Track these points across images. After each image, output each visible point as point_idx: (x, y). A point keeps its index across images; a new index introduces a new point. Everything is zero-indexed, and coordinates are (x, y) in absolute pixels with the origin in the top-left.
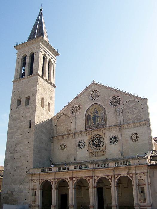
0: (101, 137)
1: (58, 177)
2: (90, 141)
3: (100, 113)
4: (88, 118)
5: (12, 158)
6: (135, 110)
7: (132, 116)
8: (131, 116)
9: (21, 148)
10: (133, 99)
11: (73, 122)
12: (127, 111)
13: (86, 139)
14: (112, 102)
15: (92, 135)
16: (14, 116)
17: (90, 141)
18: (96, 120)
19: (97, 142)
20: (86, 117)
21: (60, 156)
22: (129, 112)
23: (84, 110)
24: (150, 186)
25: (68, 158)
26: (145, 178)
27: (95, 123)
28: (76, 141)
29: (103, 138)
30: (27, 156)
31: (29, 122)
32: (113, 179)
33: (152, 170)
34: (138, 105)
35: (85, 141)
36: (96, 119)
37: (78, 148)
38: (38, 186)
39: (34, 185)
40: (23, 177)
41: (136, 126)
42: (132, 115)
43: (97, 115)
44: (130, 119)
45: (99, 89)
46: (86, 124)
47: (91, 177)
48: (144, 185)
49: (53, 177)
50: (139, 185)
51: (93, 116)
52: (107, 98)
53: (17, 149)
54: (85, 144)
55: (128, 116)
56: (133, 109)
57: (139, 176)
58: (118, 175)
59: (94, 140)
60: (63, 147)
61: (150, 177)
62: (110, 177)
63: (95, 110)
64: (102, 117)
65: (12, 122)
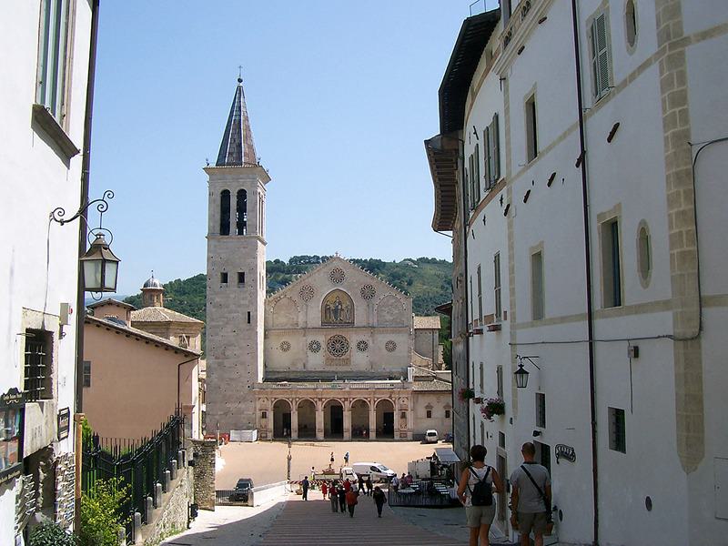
3: (344, 306)
4: (326, 310)
8: (388, 317)
13: (322, 339)
16: (217, 300)
19: (338, 346)
21: (283, 361)
25: (294, 364)
26: (410, 404)
32: (372, 402)
37: (309, 352)
38: (270, 406)
39: (261, 405)
41: (393, 332)
47: (346, 399)
49: (293, 396)
60: (286, 347)
65: (214, 310)
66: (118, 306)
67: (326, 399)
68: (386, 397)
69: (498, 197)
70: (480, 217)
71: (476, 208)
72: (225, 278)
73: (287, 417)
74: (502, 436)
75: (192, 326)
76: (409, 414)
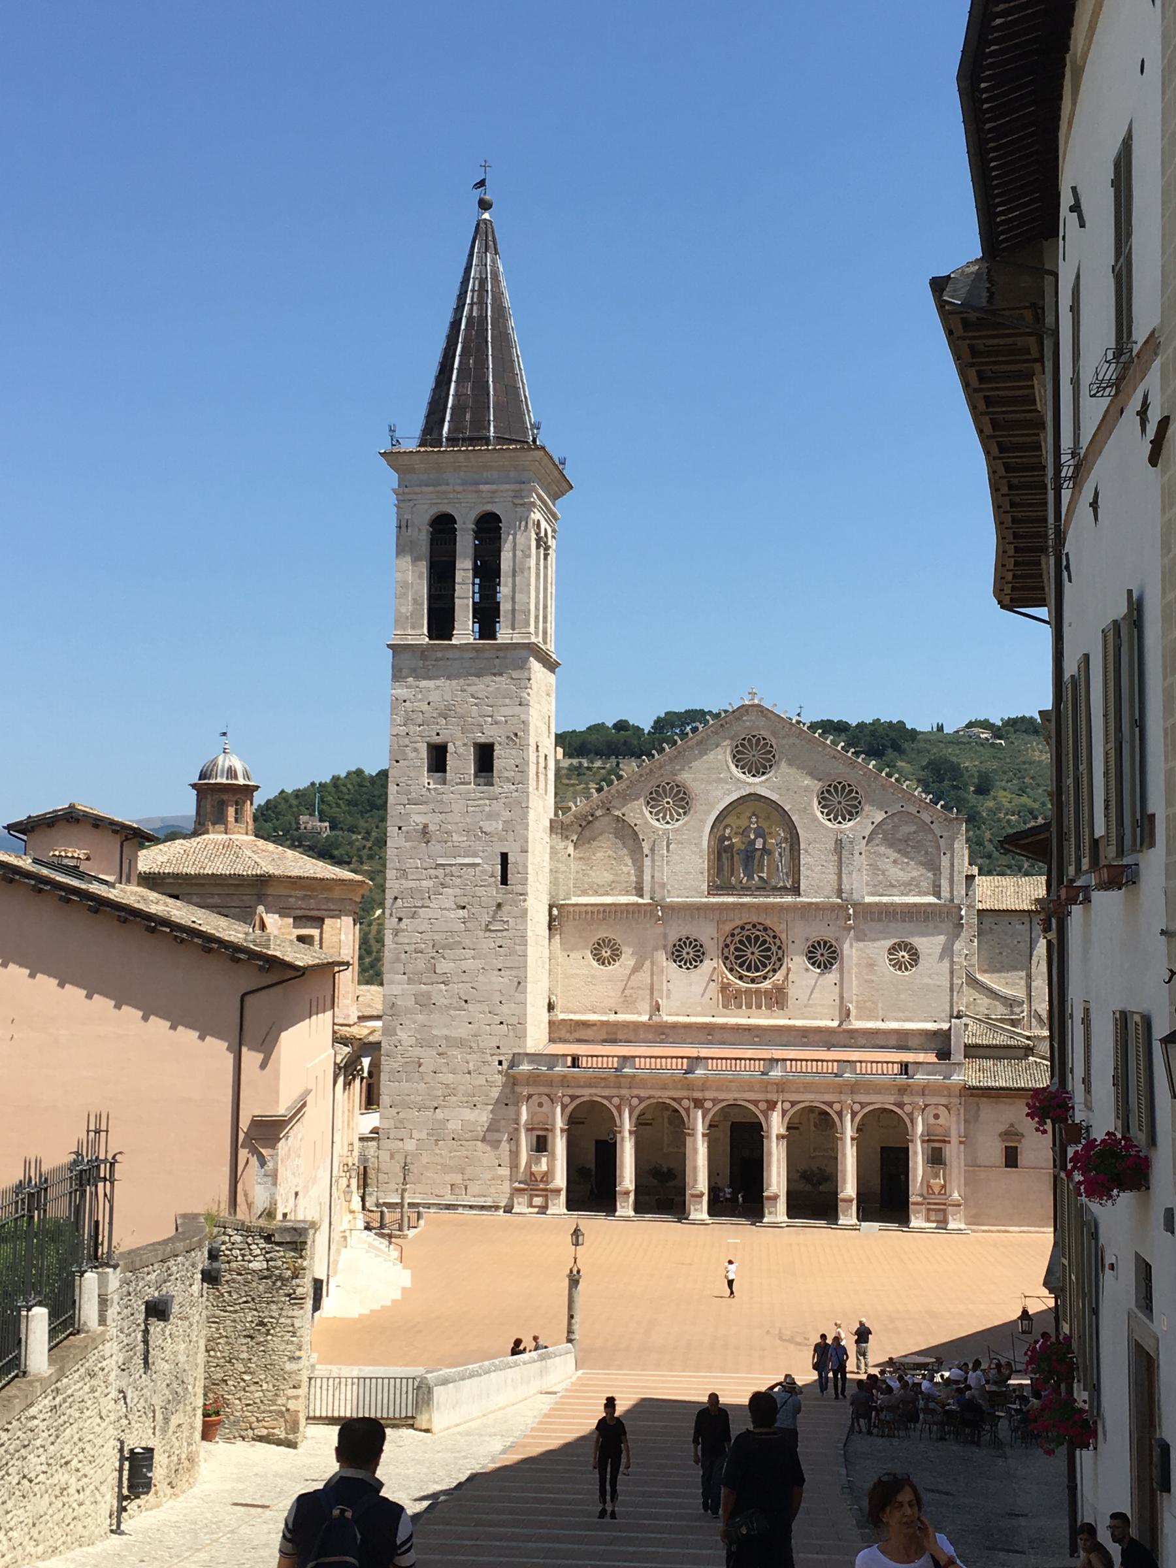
0: (772, 934)
1: (643, 1093)
2: (727, 946)
5: (424, 1003)
7: (901, 873)
9: (464, 965)
15: (739, 923)
17: (727, 946)
18: (755, 867)
22: (892, 859)
23: (708, 812)
24: (962, 1146)
26: (952, 1124)
27: (751, 878)
28: (665, 936)
29: (777, 940)
30: (497, 997)
31: (499, 861)
33: (976, 1099)
34: (930, 837)
35: (704, 939)
36: (756, 862)
40: (481, 1080)
43: (759, 844)
44: (894, 886)
45: (774, 734)
48: (949, 1142)
50: (928, 1141)
51: (743, 848)
52: (806, 782)
53: (443, 966)
54: (703, 954)
57: (936, 1112)
58: (863, 1105)
59: (741, 942)
61: (965, 1121)
62: (837, 1107)
63: (754, 819)
64: (780, 854)
65: (408, 844)
66: (96, 826)
67: (715, 1101)
68: (886, 1101)
69: (1135, 404)
70: (1087, 495)
71: (1078, 478)
72: (438, 758)
73: (607, 1153)
74: (1145, 1272)
75: (330, 889)
76: (953, 1152)
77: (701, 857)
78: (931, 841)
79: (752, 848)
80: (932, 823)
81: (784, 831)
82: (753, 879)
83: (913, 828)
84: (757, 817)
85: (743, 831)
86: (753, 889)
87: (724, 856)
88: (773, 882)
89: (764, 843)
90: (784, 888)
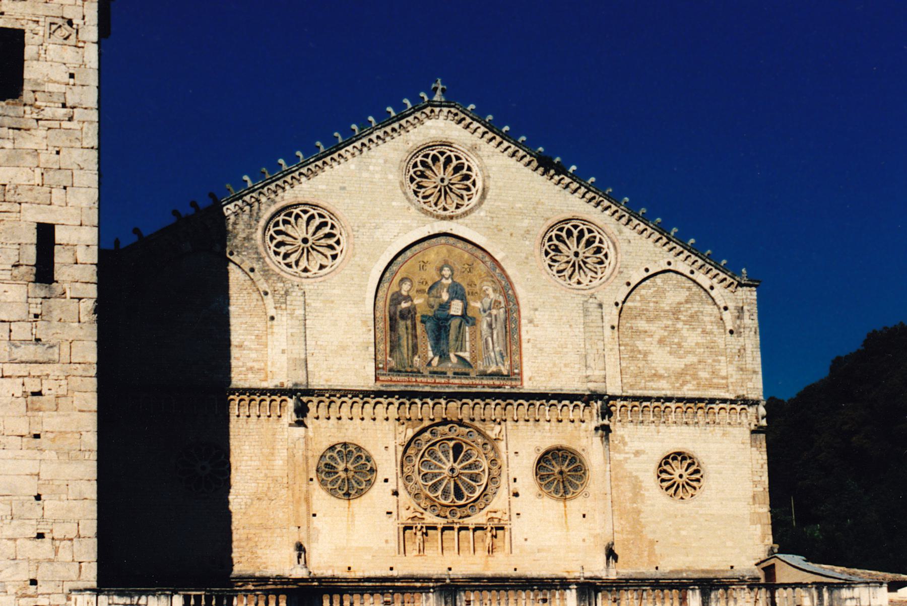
6: (685, 332)
7: (672, 359)
10: (684, 268)
11: (282, 319)
12: (642, 324)
14: (553, 251)
15: (426, 423)
18: (452, 343)
20: (380, 304)
22: (657, 337)
27: (444, 357)
34: (709, 308)
42: (670, 353)
43: (456, 308)
44: (661, 377)
46: (381, 347)
55: (646, 354)
56: (680, 325)
63: (446, 272)
64: (490, 326)
77: (364, 322)
78: (711, 315)
79: (441, 314)
80: (712, 288)
81: (495, 290)
82: (449, 359)
83: (683, 295)
84: (452, 270)
85: (431, 288)
86: (450, 374)
87: (402, 324)
88: (481, 366)
89: (465, 308)
90: (498, 375)
